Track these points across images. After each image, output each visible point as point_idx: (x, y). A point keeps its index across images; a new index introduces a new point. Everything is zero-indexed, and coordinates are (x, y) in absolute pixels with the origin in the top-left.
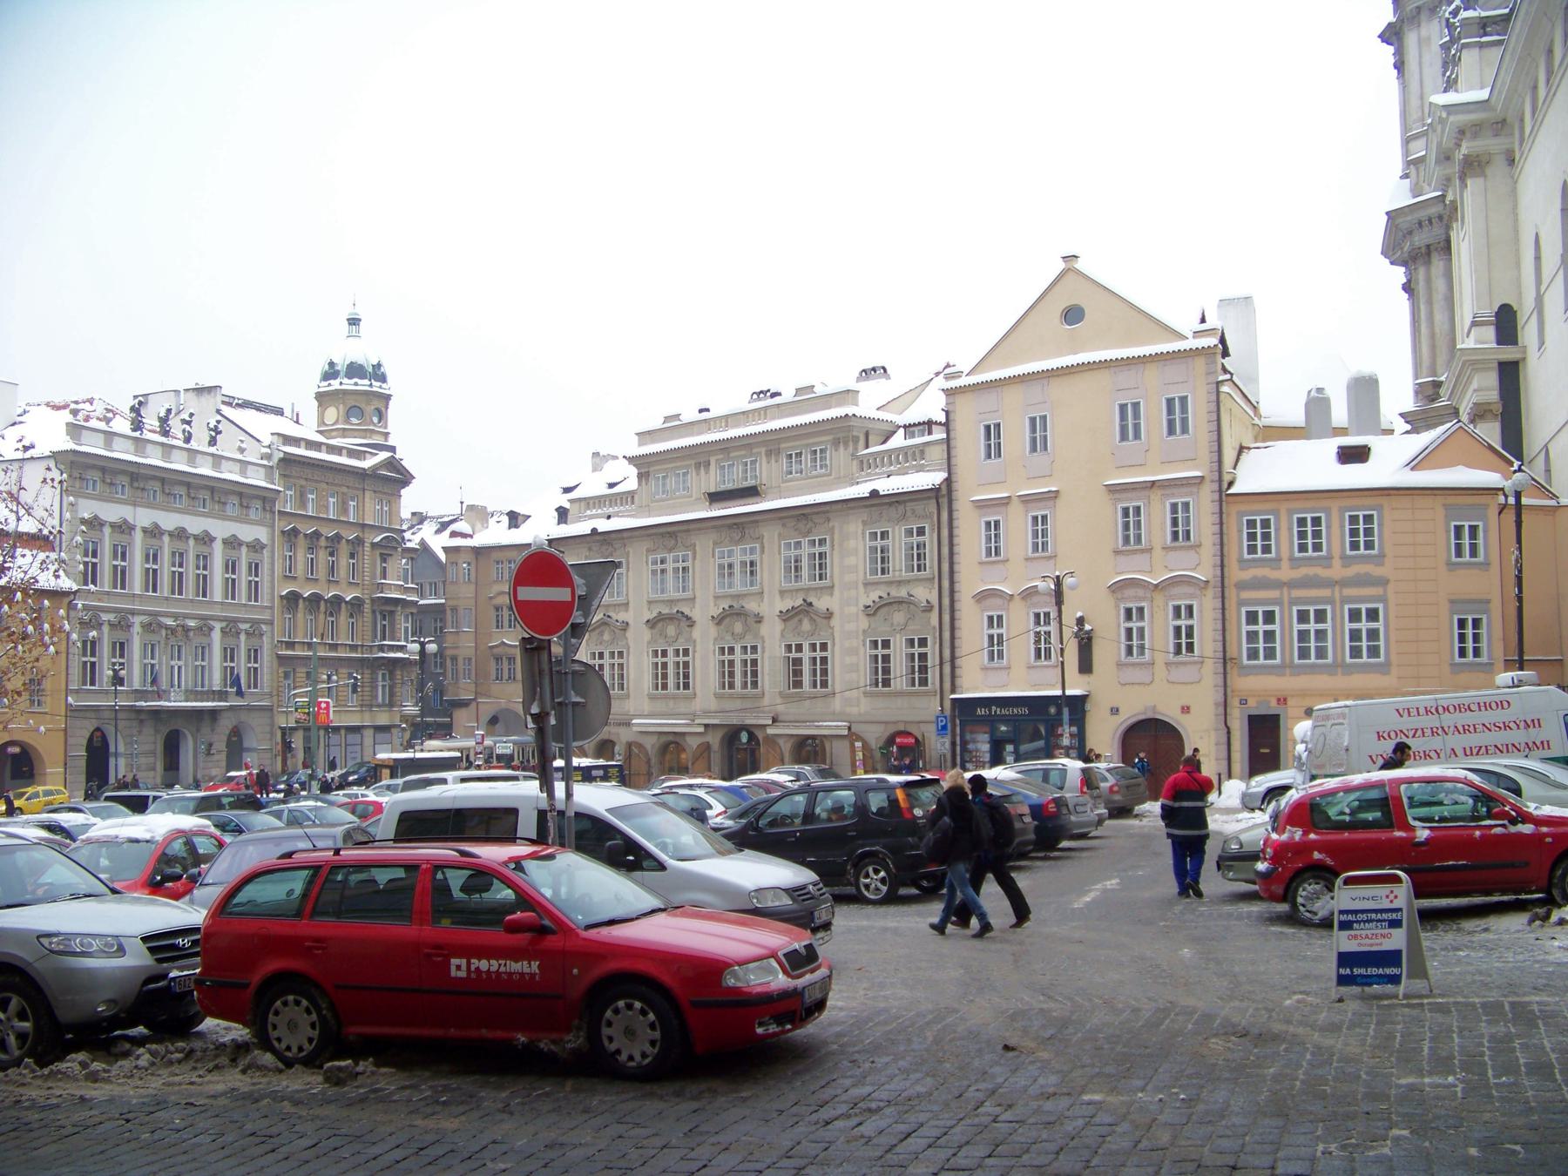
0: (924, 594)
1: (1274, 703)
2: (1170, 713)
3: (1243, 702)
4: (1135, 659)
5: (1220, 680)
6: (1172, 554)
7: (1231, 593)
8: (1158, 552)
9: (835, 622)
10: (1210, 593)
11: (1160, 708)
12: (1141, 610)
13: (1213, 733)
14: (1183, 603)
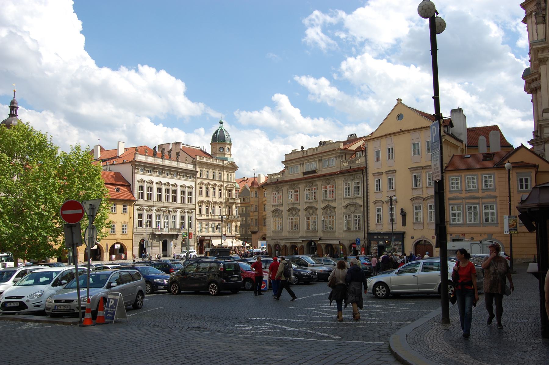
0: (360, 202)
1: (461, 235)
3: (451, 235)
8: (424, 189)
9: (336, 210)
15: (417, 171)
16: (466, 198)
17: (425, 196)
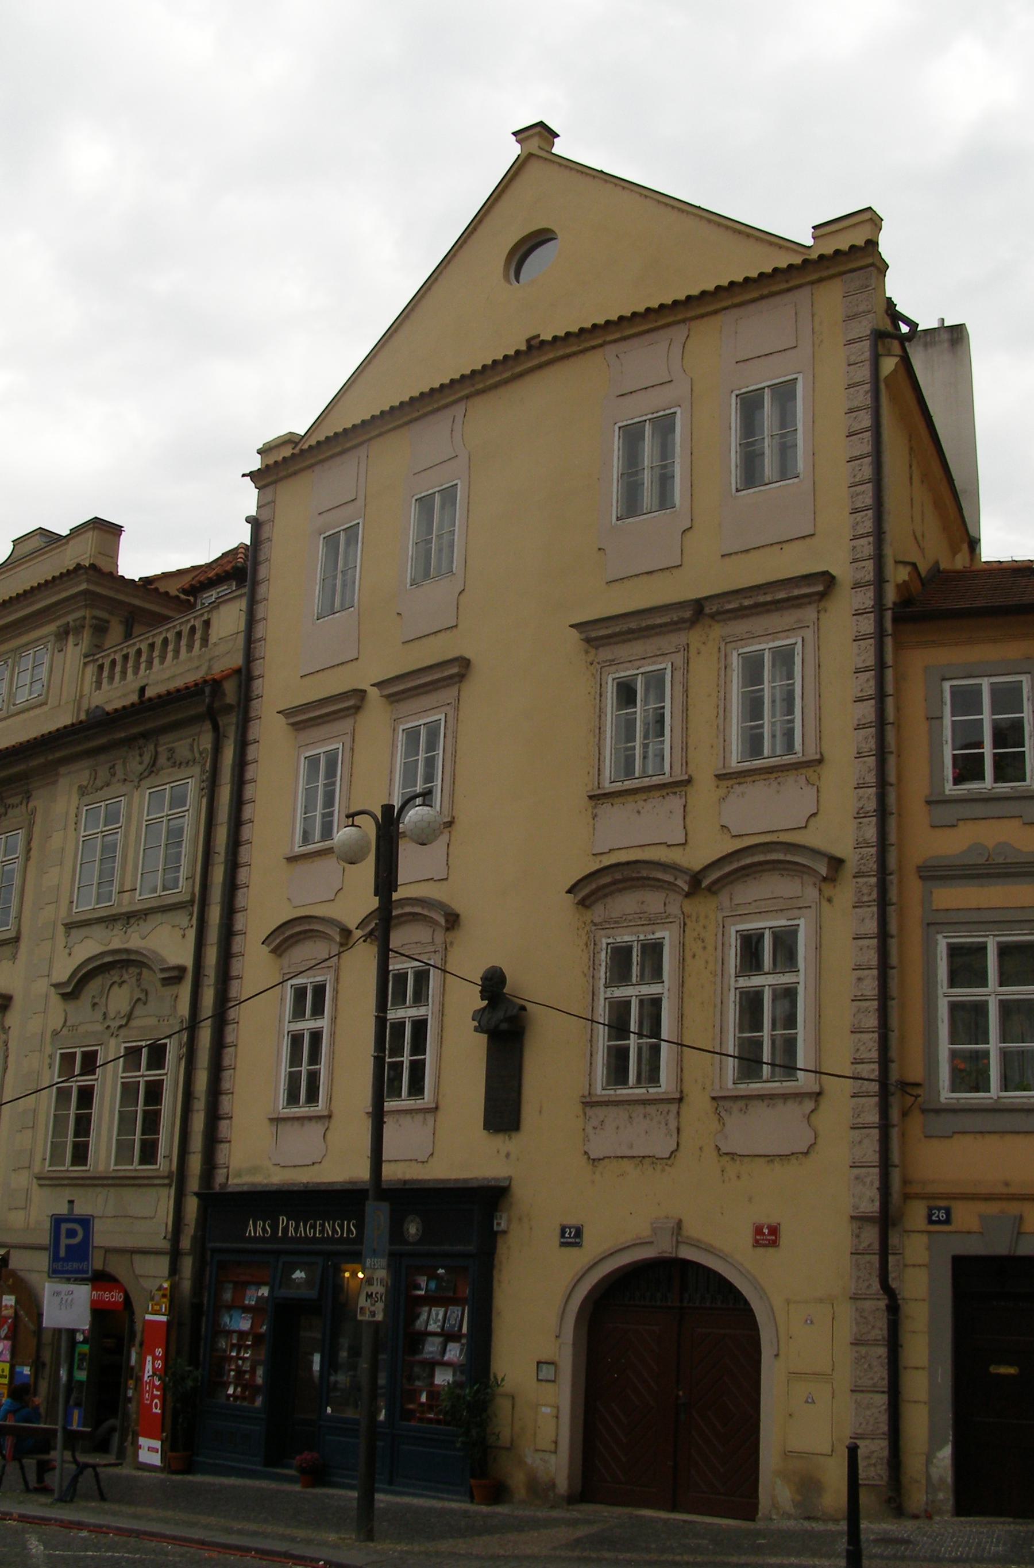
0: (171, 944)
2: (721, 1241)
3: (940, 1216)
4: (632, 1091)
5: (870, 1150)
8: (705, 789)
10: (845, 892)
11: (692, 1229)
12: (653, 951)
13: (846, 1312)
15: (637, 648)
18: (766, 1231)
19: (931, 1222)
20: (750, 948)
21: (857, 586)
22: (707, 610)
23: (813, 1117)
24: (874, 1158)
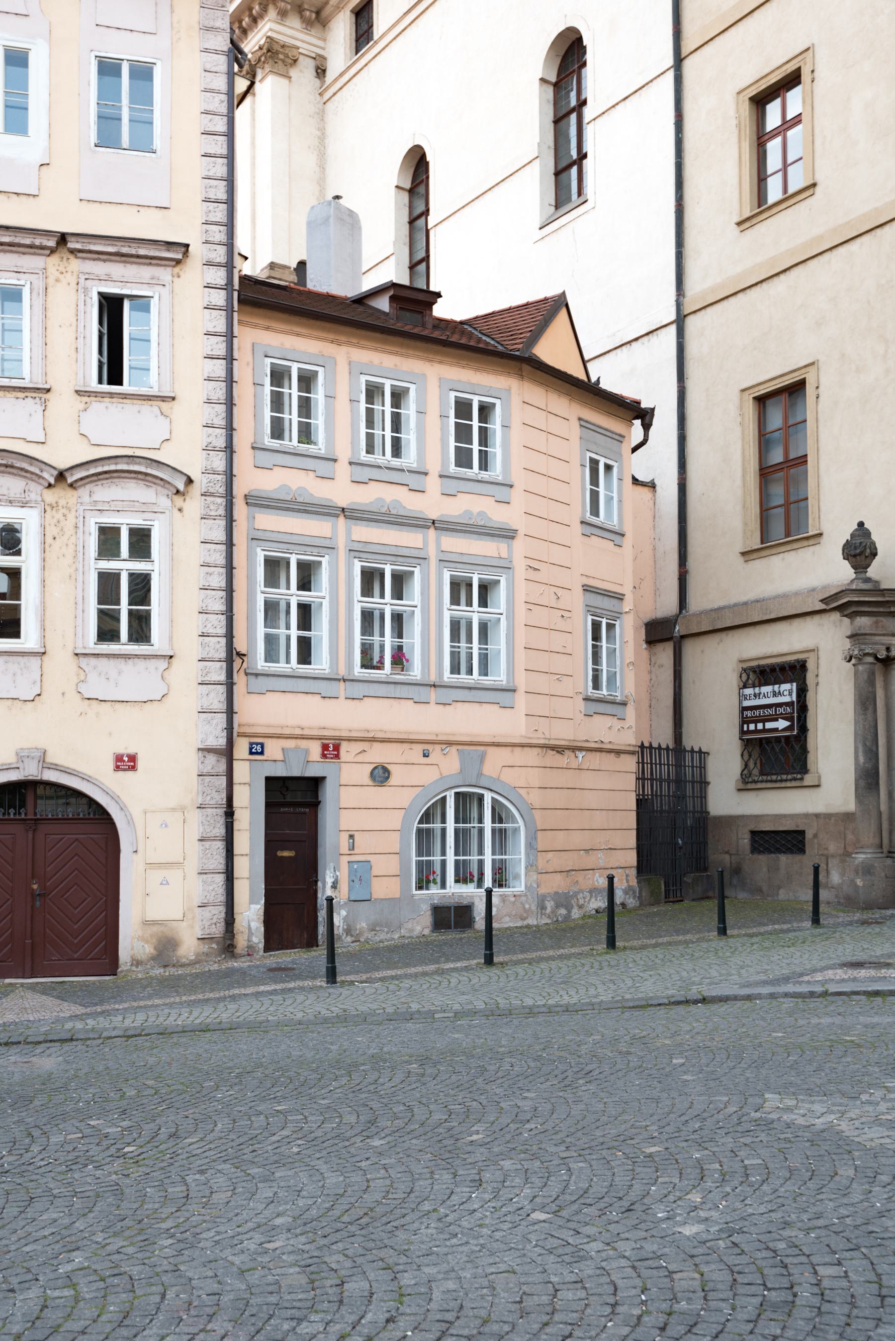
1: (315, 749)
3: (256, 750)
5: (217, 698)
6: (97, 406)
7: (241, 510)
10: (194, 505)
13: (195, 818)
14: (125, 522)
16: (347, 513)
17: (64, 453)
18: (126, 759)
19: (251, 753)
20: (108, 539)
21: (209, 264)
22: (71, 245)
23: (166, 674)
24: (223, 707)
